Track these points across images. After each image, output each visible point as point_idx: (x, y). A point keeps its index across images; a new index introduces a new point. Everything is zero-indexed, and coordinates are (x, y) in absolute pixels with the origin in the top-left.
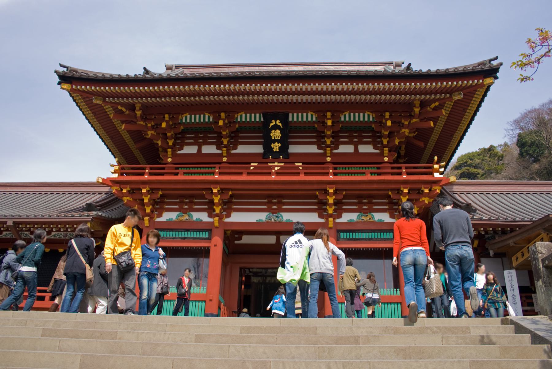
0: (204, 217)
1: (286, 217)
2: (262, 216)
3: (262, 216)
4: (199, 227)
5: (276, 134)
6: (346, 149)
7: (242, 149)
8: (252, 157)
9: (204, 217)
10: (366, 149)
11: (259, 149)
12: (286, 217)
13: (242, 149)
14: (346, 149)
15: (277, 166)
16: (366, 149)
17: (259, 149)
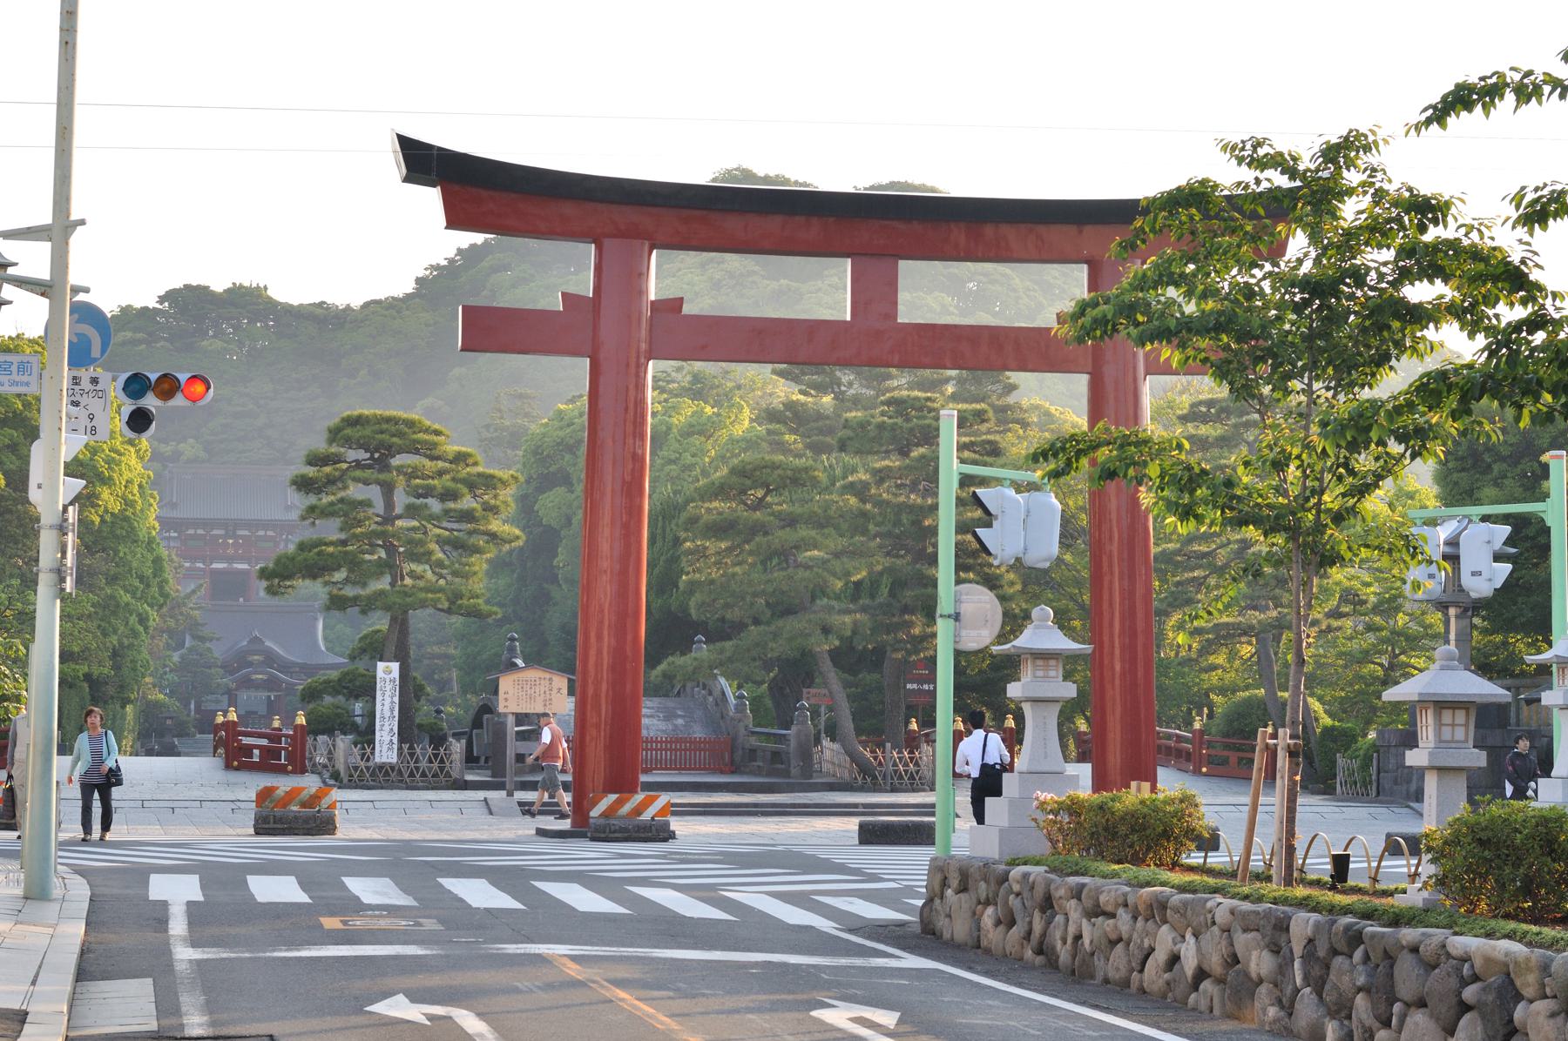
0: (201, 565)
1: (235, 565)
2: (225, 565)
3: (225, 565)
4: (200, 569)
5: (231, 528)
6: (261, 533)
7: (215, 532)
8: (220, 536)
9: (201, 565)
10: (270, 533)
11: (221, 532)
12: (235, 565)
13: (215, 532)
14: (261, 533)
15: (231, 541)
16: (270, 533)
17: (221, 532)
